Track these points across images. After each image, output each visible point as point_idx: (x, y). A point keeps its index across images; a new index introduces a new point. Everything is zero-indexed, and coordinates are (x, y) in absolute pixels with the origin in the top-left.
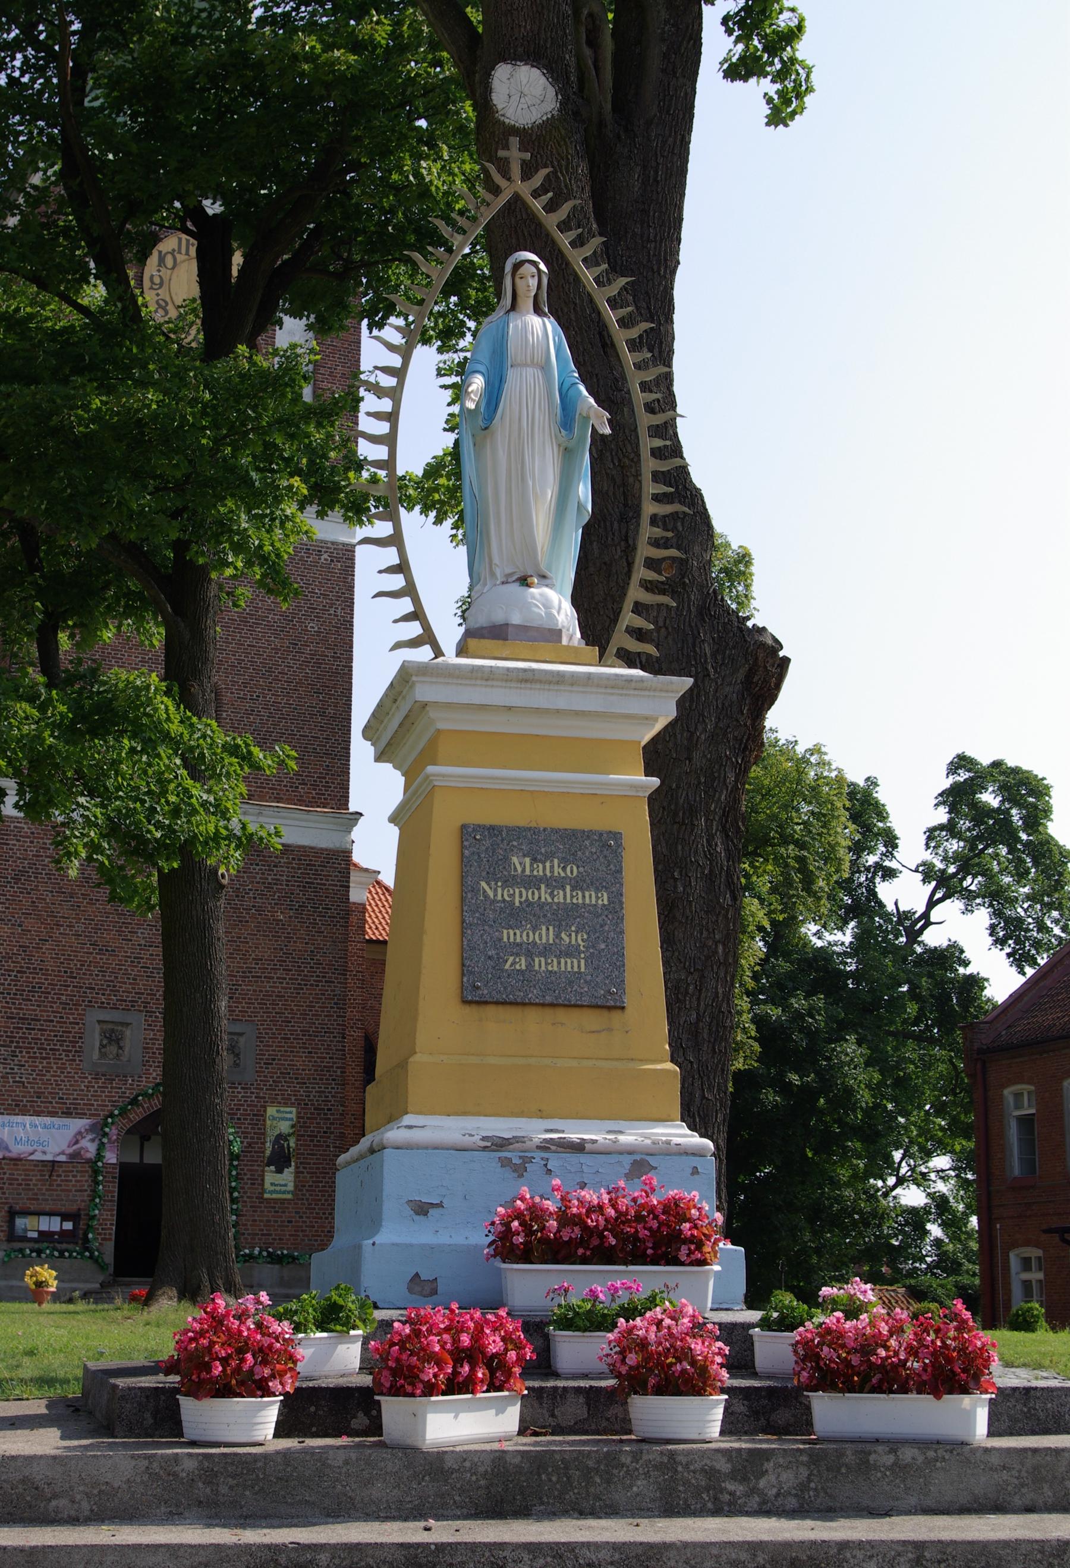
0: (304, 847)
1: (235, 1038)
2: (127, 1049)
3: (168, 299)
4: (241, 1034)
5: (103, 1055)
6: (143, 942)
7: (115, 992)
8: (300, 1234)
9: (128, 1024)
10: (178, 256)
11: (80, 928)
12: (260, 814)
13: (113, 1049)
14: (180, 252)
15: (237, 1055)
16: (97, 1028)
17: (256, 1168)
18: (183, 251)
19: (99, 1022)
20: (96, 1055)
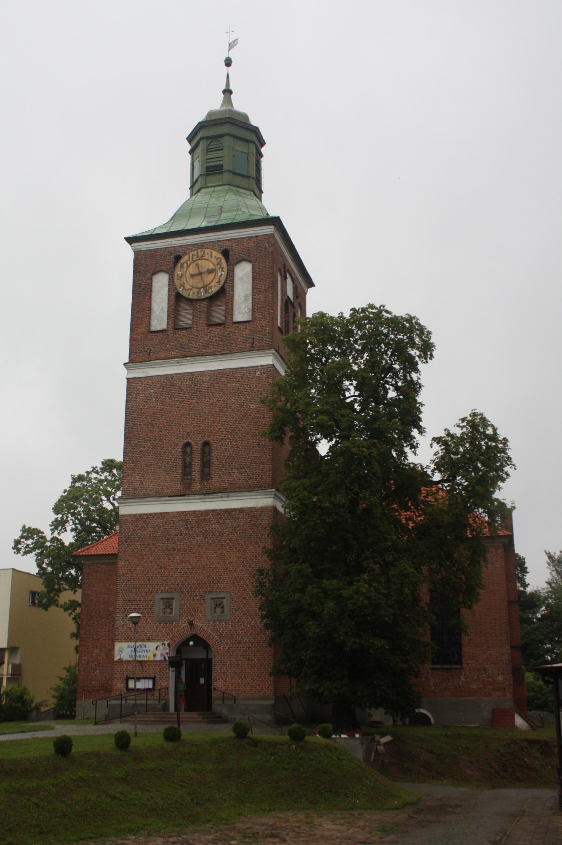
0: (250, 508)
1: (222, 600)
2: (174, 609)
3: (185, 282)
4: (224, 598)
5: (164, 613)
6: (179, 562)
7: (167, 585)
8: (254, 689)
9: (173, 599)
10: (189, 263)
11: (152, 558)
12: (228, 497)
13: (168, 610)
14: (189, 260)
15: (223, 607)
16: (161, 601)
17: (232, 659)
18: (191, 259)
19: (162, 599)
20: (161, 614)
